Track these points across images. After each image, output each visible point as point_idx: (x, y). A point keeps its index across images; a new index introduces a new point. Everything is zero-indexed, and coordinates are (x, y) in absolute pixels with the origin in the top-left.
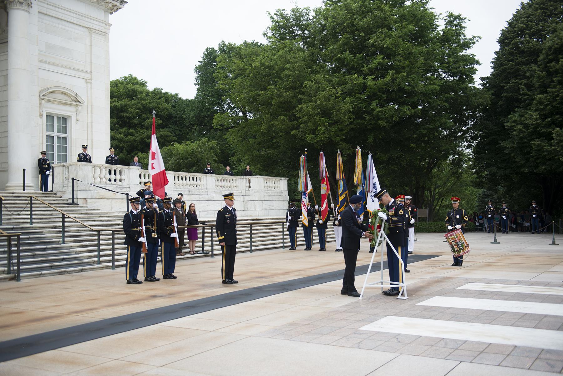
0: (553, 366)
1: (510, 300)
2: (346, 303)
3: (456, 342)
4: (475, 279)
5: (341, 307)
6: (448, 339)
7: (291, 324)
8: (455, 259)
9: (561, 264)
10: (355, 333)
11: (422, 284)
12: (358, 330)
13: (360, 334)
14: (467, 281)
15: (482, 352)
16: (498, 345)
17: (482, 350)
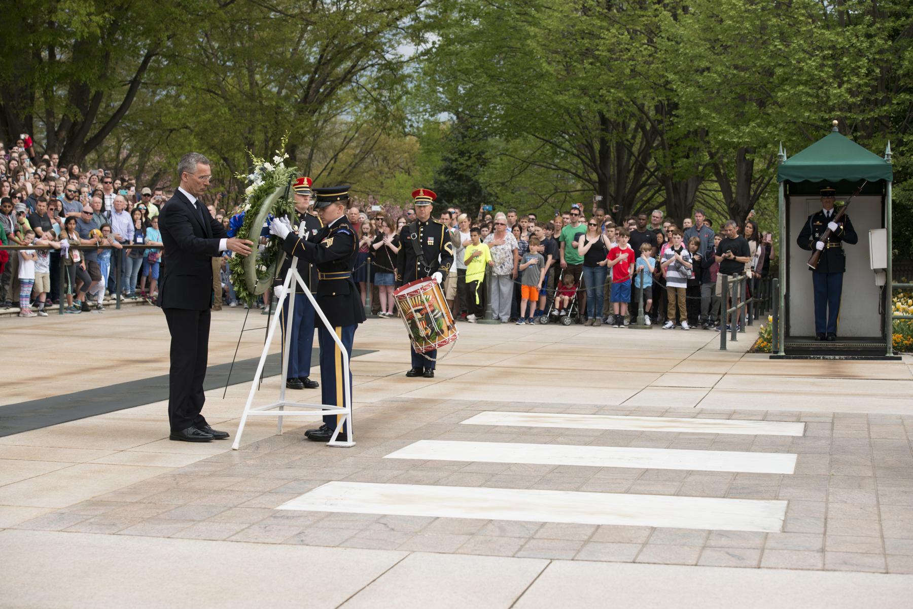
0: (740, 558)
1: (598, 445)
2: (203, 458)
3: (524, 527)
4: (492, 403)
5: (195, 465)
6: (502, 521)
7: (93, 503)
8: (416, 356)
9: (673, 370)
10: (275, 517)
11: (367, 416)
12: (278, 511)
13: (288, 518)
14: (476, 408)
15: (587, 542)
16: (616, 528)
17: (586, 537)
